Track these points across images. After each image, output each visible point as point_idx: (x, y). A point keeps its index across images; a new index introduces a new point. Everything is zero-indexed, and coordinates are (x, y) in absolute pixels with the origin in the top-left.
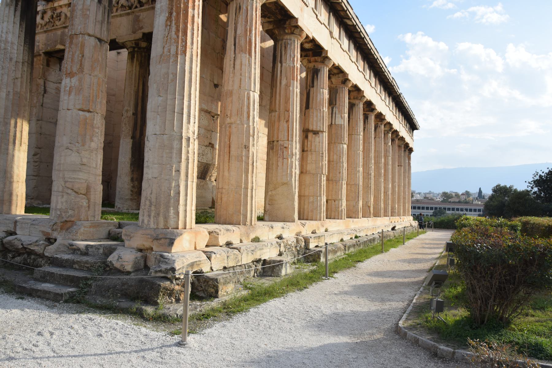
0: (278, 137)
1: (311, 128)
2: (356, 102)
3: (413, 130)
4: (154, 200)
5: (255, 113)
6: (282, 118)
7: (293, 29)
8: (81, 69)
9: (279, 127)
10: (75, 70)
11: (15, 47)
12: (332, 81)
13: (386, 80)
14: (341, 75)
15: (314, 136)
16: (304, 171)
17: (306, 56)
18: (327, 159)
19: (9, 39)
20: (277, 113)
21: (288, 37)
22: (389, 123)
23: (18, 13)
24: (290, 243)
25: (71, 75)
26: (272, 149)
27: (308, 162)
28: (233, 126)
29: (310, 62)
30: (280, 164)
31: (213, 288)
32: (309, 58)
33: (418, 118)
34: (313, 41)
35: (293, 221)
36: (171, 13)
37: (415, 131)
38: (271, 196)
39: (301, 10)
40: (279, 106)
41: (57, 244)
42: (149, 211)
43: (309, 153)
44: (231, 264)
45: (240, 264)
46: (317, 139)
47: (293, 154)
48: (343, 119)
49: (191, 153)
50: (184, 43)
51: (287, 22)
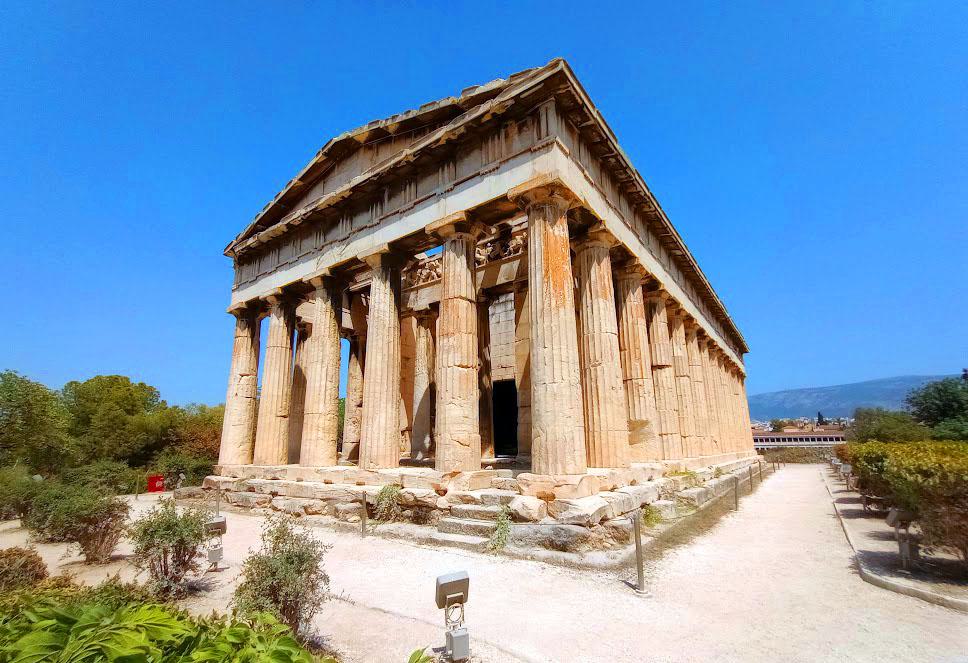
2: (690, 331)
10: (451, 330)
11: (387, 315)
21: (630, 276)
22: (721, 350)
30: (636, 403)
36: (547, 271)
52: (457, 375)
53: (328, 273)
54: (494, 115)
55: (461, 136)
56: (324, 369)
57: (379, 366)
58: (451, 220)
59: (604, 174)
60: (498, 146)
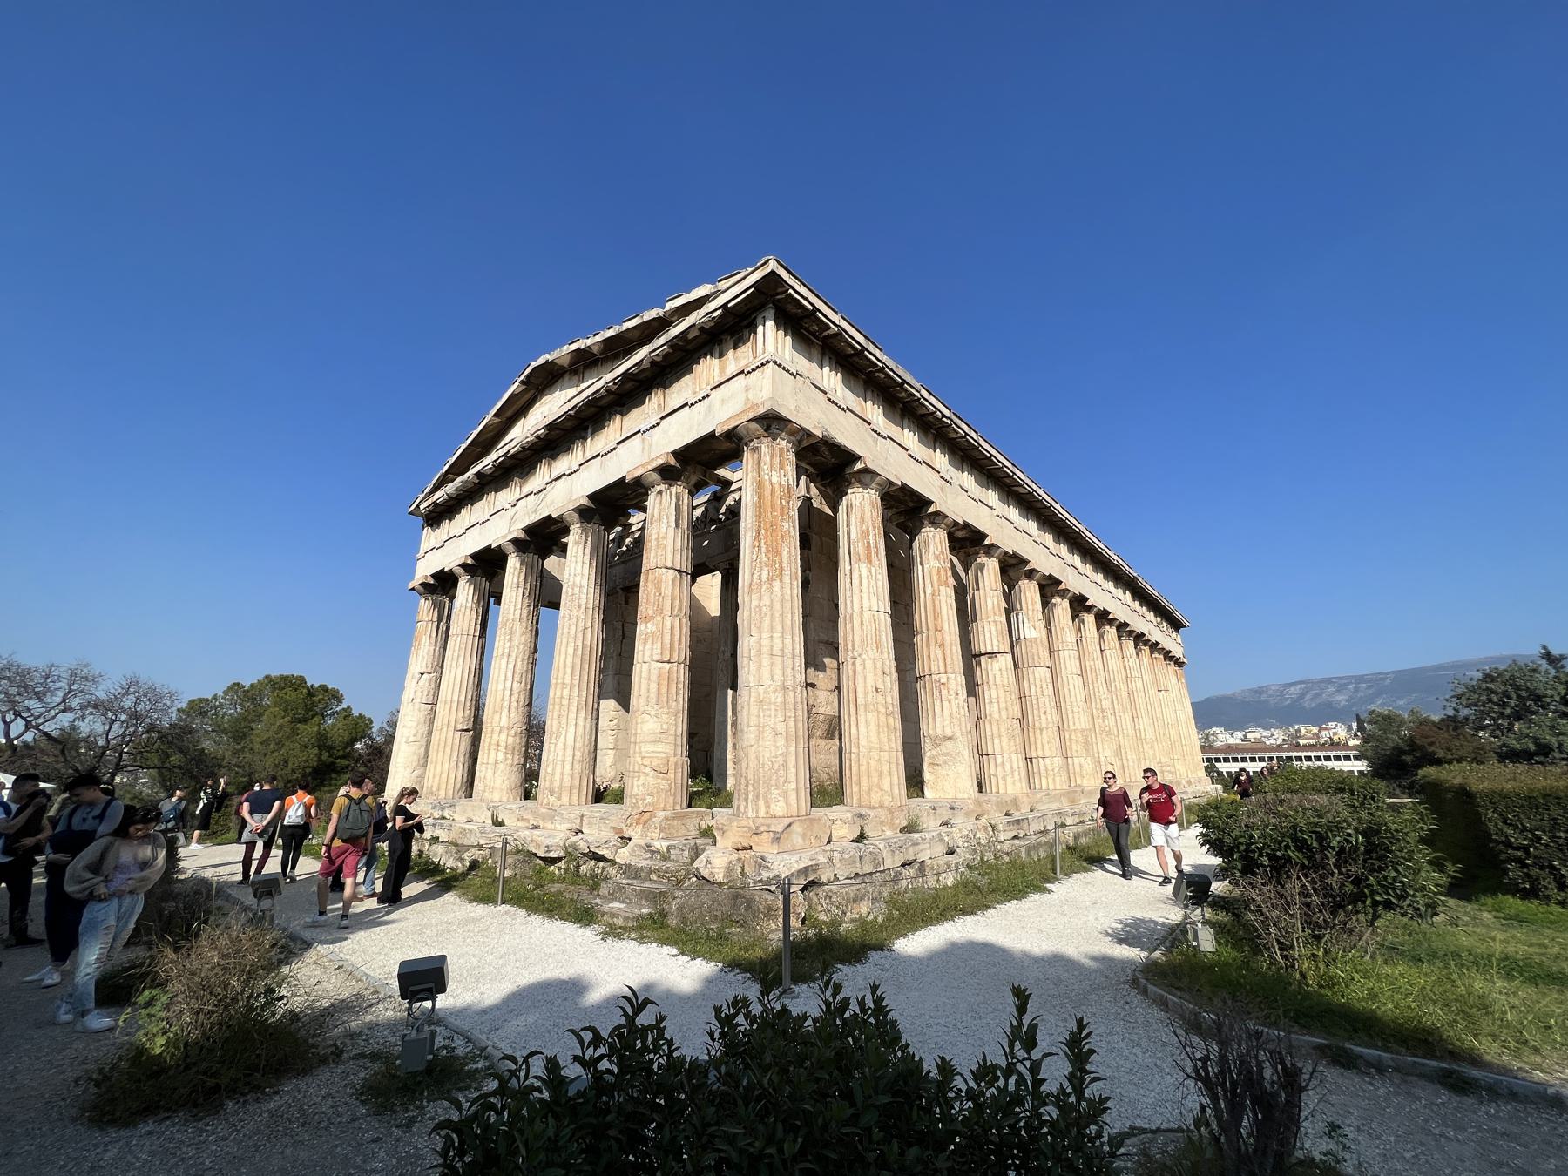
4: (750, 776)
6: (932, 642)
8: (660, 611)
19: (578, 579)
23: (588, 550)
25: (646, 619)
28: (858, 662)
30: (937, 709)
34: (967, 525)
36: (758, 532)
38: (933, 757)
41: (631, 844)
42: (747, 794)
44: (867, 870)
46: (996, 666)
52: (654, 678)
53: (522, 535)
54: (702, 329)
55: (666, 356)
56: (511, 666)
57: (570, 660)
58: (654, 465)
60: (708, 369)
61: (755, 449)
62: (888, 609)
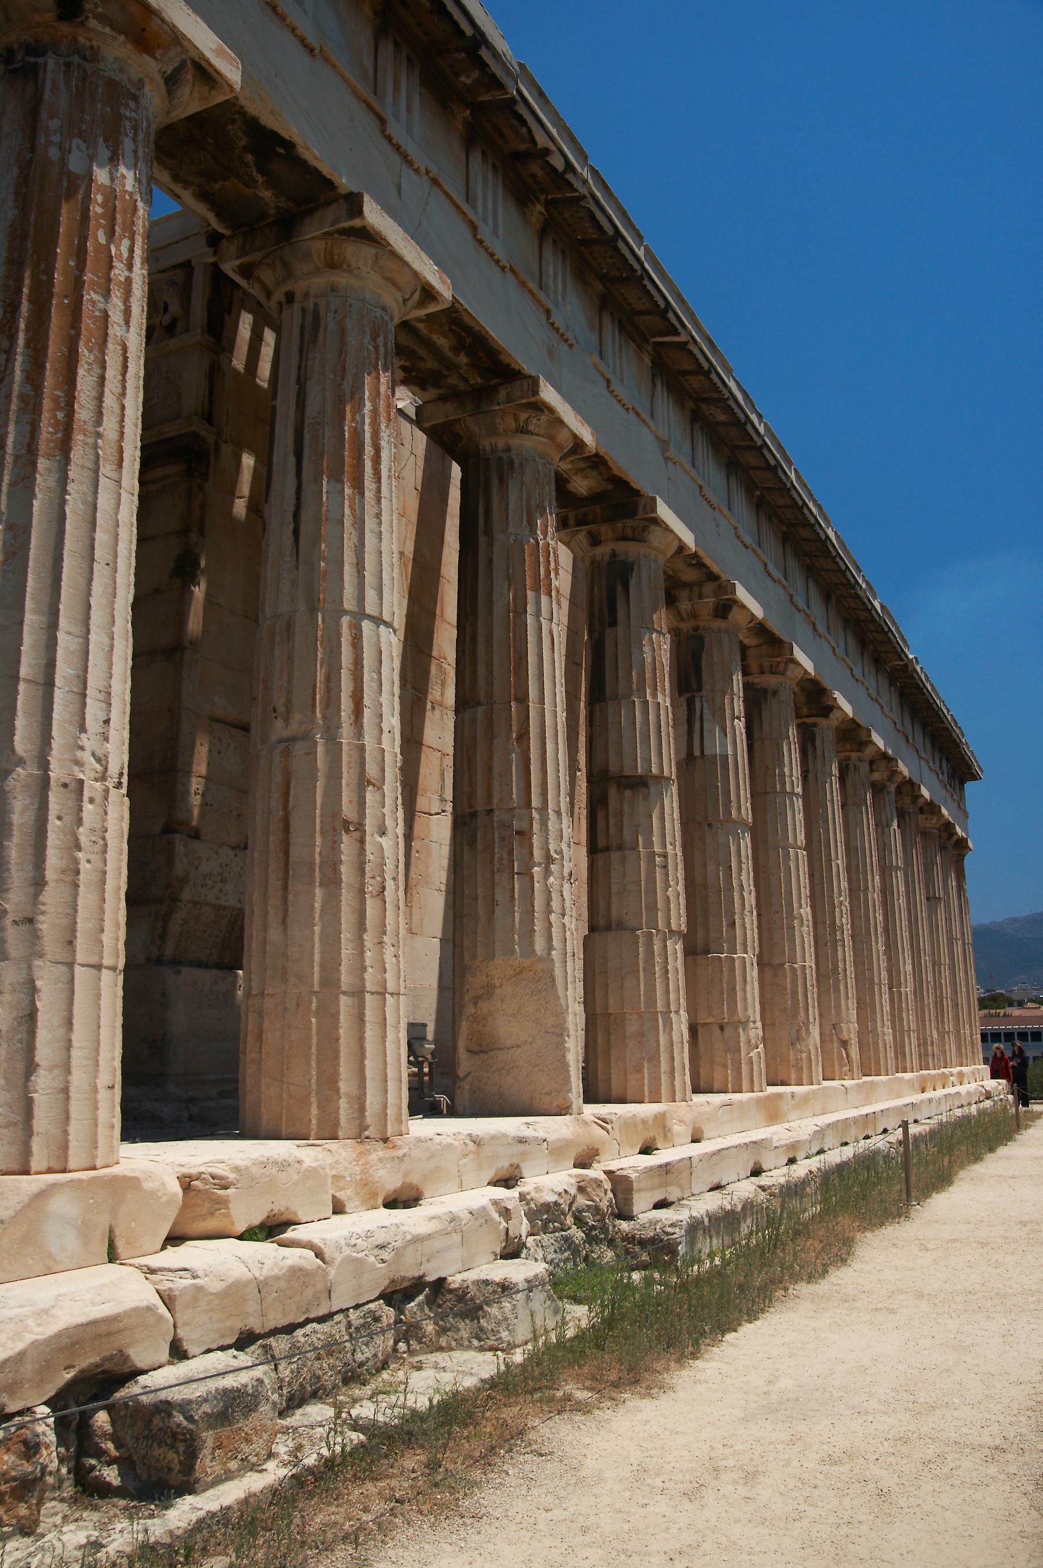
0: (489, 797)
1: (613, 768)
3: (962, 783)
5: (384, 699)
7: (523, 416)
9: (490, 759)
12: (679, 613)
13: (862, 615)
14: (708, 588)
15: (628, 793)
16: (602, 922)
17: (580, 523)
18: (681, 874)
20: (481, 710)
24: (551, 1198)
26: (473, 842)
27: (614, 888)
29: (595, 541)
31: (172, 1447)
32: (593, 527)
33: (975, 741)
35: (563, 1110)
37: (969, 786)
39: (550, 352)
40: (490, 683)
43: (615, 855)
45: (322, 1311)
47: (549, 859)
48: (731, 739)
49: (111, 855)
50: (60, 415)
51: (502, 394)
59: (387, 49)
61: (31, 73)
62: (399, 622)
